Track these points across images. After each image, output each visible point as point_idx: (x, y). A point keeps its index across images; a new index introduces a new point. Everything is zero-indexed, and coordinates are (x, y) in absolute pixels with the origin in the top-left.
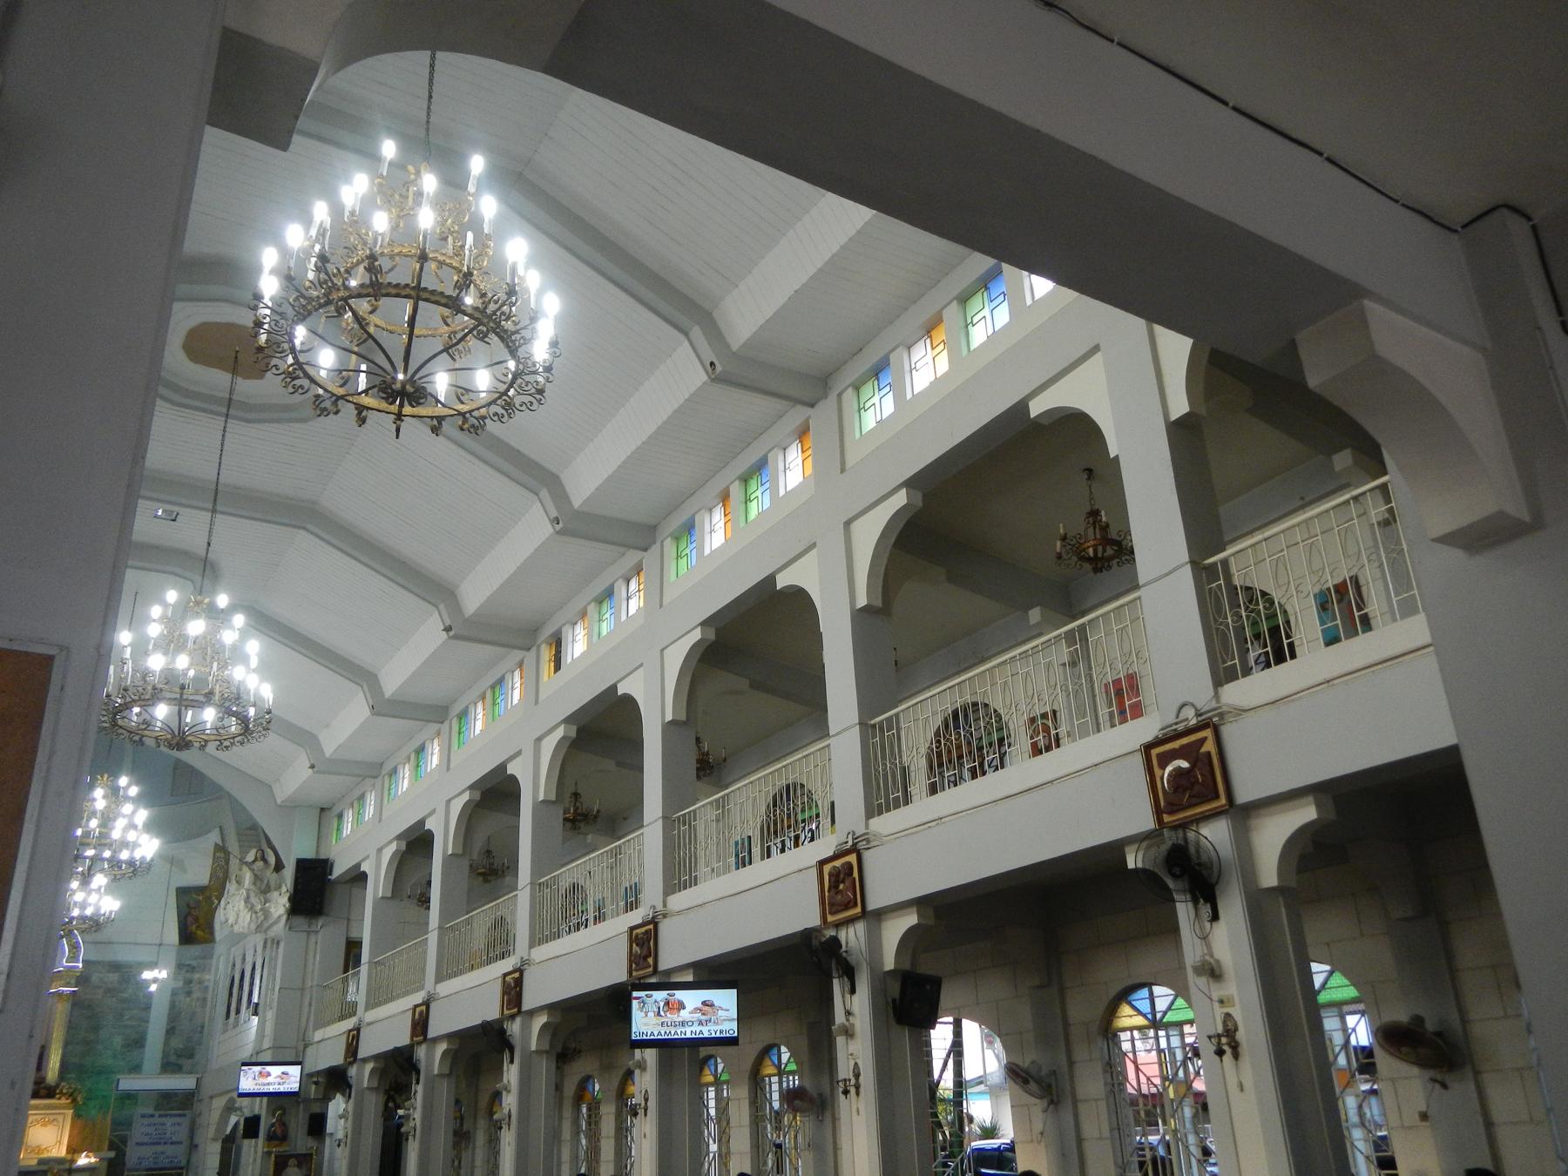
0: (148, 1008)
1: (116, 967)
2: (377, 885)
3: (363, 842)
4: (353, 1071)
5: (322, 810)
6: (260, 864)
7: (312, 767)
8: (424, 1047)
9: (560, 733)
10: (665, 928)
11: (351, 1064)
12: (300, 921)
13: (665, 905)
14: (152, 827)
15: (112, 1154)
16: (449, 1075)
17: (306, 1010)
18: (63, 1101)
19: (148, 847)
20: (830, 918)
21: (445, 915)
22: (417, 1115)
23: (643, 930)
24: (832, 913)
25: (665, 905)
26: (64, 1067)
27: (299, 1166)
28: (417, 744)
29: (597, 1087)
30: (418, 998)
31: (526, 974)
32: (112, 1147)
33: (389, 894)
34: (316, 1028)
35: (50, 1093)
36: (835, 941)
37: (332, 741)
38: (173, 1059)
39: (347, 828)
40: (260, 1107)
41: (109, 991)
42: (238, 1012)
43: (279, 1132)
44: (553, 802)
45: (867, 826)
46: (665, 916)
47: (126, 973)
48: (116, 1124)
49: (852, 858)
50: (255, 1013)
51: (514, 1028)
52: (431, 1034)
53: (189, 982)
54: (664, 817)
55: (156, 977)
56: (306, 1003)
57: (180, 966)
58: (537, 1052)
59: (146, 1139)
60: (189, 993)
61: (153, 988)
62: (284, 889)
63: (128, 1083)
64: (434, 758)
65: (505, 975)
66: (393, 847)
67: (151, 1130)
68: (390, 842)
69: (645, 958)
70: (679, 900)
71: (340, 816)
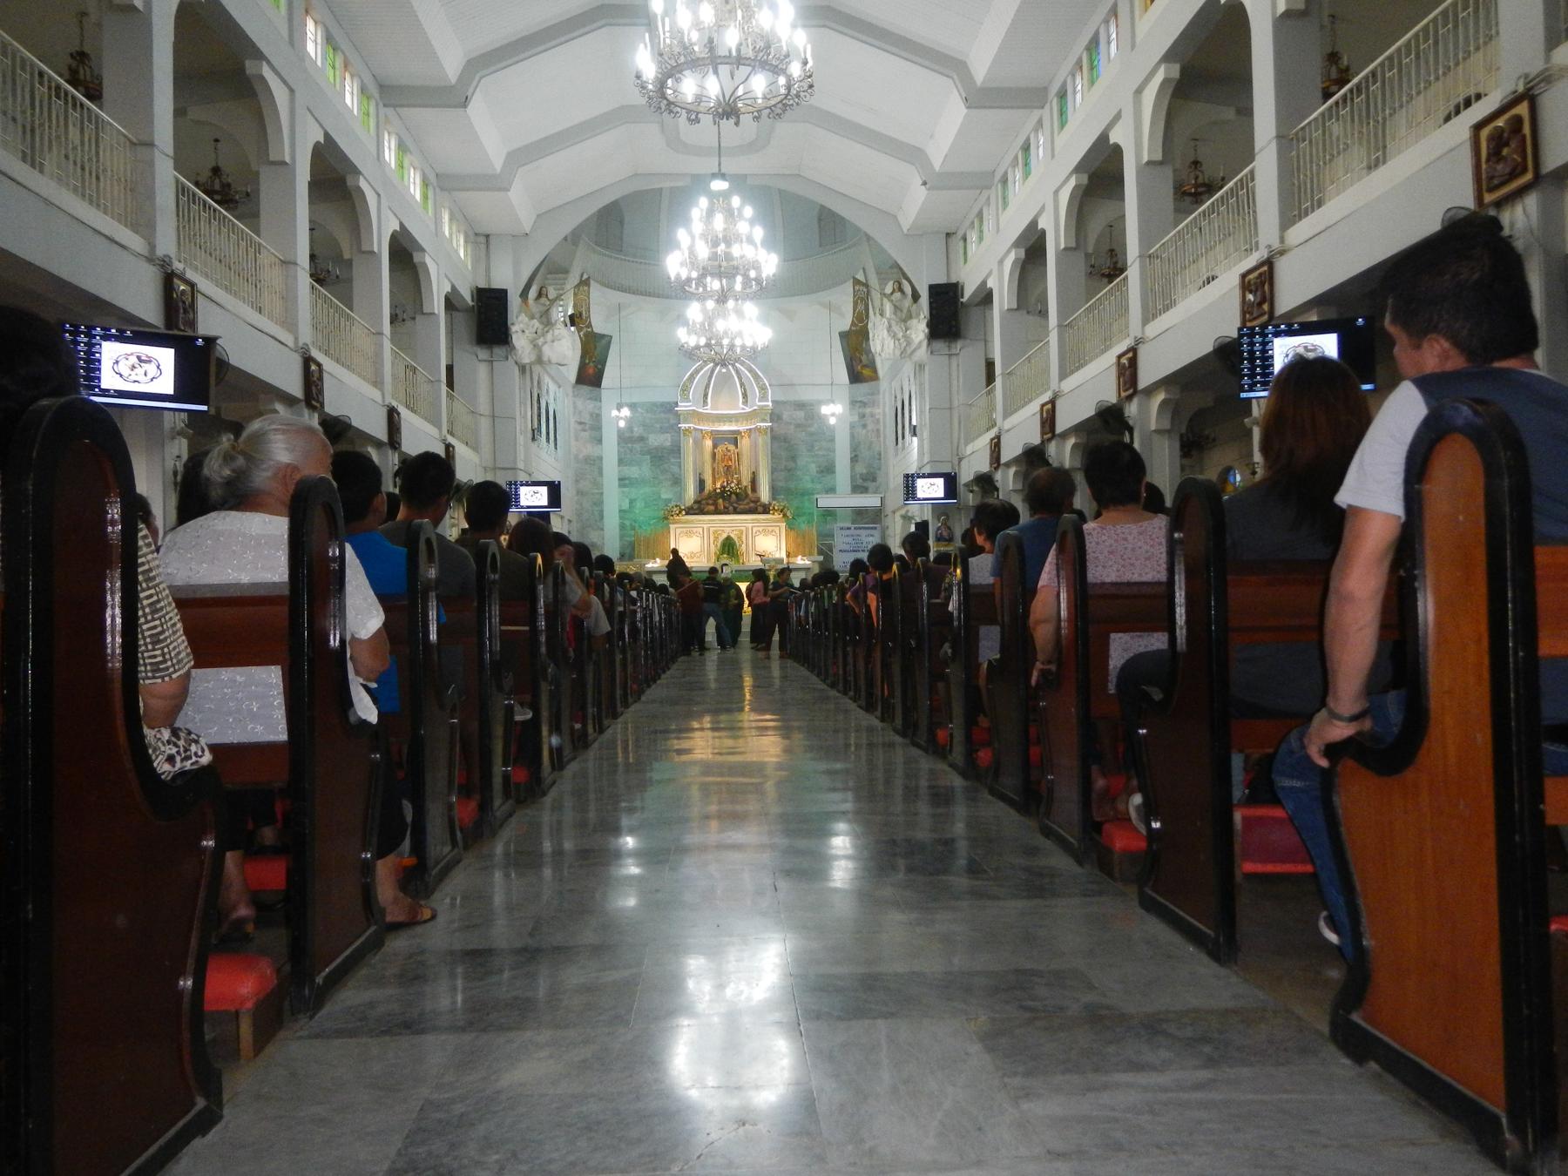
0: (832, 440)
1: (801, 405)
2: (1003, 299)
4: (998, 476)
5: (948, 235)
6: (898, 295)
7: (925, 183)
8: (1053, 443)
10: (1283, 268)
12: (940, 345)
13: (1282, 240)
14: (769, 244)
15: (821, 558)
18: (777, 516)
19: (770, 264)
20: (1488, 198)
21: (1062, 314)
23: (1256, 274)
24: (1490, 190)
25: (1282, 240)
26: (774, 491)
28: (1020, 141)
29: (1238, 478)
30: (1046, 397)
32: (820, 552)
34: (966, 444)
35: (766, 510)
36: (1496, 224)
37: (938, 153)
38: (860, 482)
39: (972, 248)
40: (927, 515)
41: (798, 426)
44: (1161, 163)
45: (1548, 59)
46: (1282, 253)
47: (808, 409)
48: (821, 535)
49: (1522, 109)
50: (915, 434)
53: (863, 416)
54: (1279, 137)
55: (834, 412)
56: (956, 421)
57: (853, 403)
58: (1157, 431)
59: (847, 547)
60: (864, 426)
61: (832, 421)
63: (825, 501)
64: (1040, 152)
65: (1119, 357)
66: (1012, 256)
67: (850, 540)
68: (1008, 252)
69: (1260, 304)
70: (1298, 232)
71: (965, 240)
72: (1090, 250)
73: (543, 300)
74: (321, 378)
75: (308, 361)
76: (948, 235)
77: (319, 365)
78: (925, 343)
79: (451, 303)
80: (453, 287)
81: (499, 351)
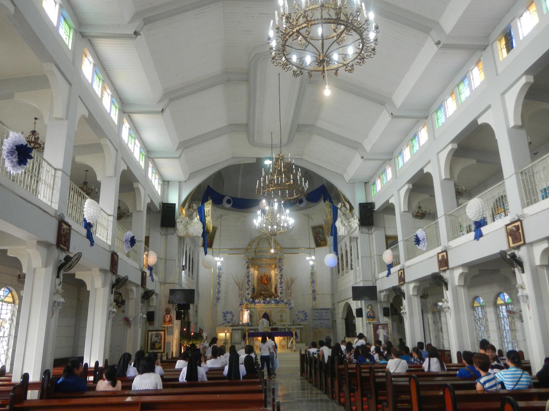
3: (389, 188)
4: (404, 288)
5: (365, 183)
9: (523, 80)
11: (403, 285)
12: (365, 229)
16: (463, 286)
17: (373, 265)
22: (450, 304)
27: (383, 328)
30: (439, 249)
31: (524, 222)
33: (407, 210)
34: (379, 273)
42: (343, 270)
43: (371, 315)
44: (521, 127)
51: (522, 253)
52: (451, 266)
56: (373, 263)
58: (541, 266)
59: (316, 318)
62: (355, 217)
65: (507, 225)
66: (406, 187)
72: (456, 180)
73: (191, 210)
74: (69, 234)
75: (61, 222)
76: (365, 183)
77: (69, 226)
78: (358, 228)
79: (150, 208)
80: (151, 201)
81: (170, 230)
